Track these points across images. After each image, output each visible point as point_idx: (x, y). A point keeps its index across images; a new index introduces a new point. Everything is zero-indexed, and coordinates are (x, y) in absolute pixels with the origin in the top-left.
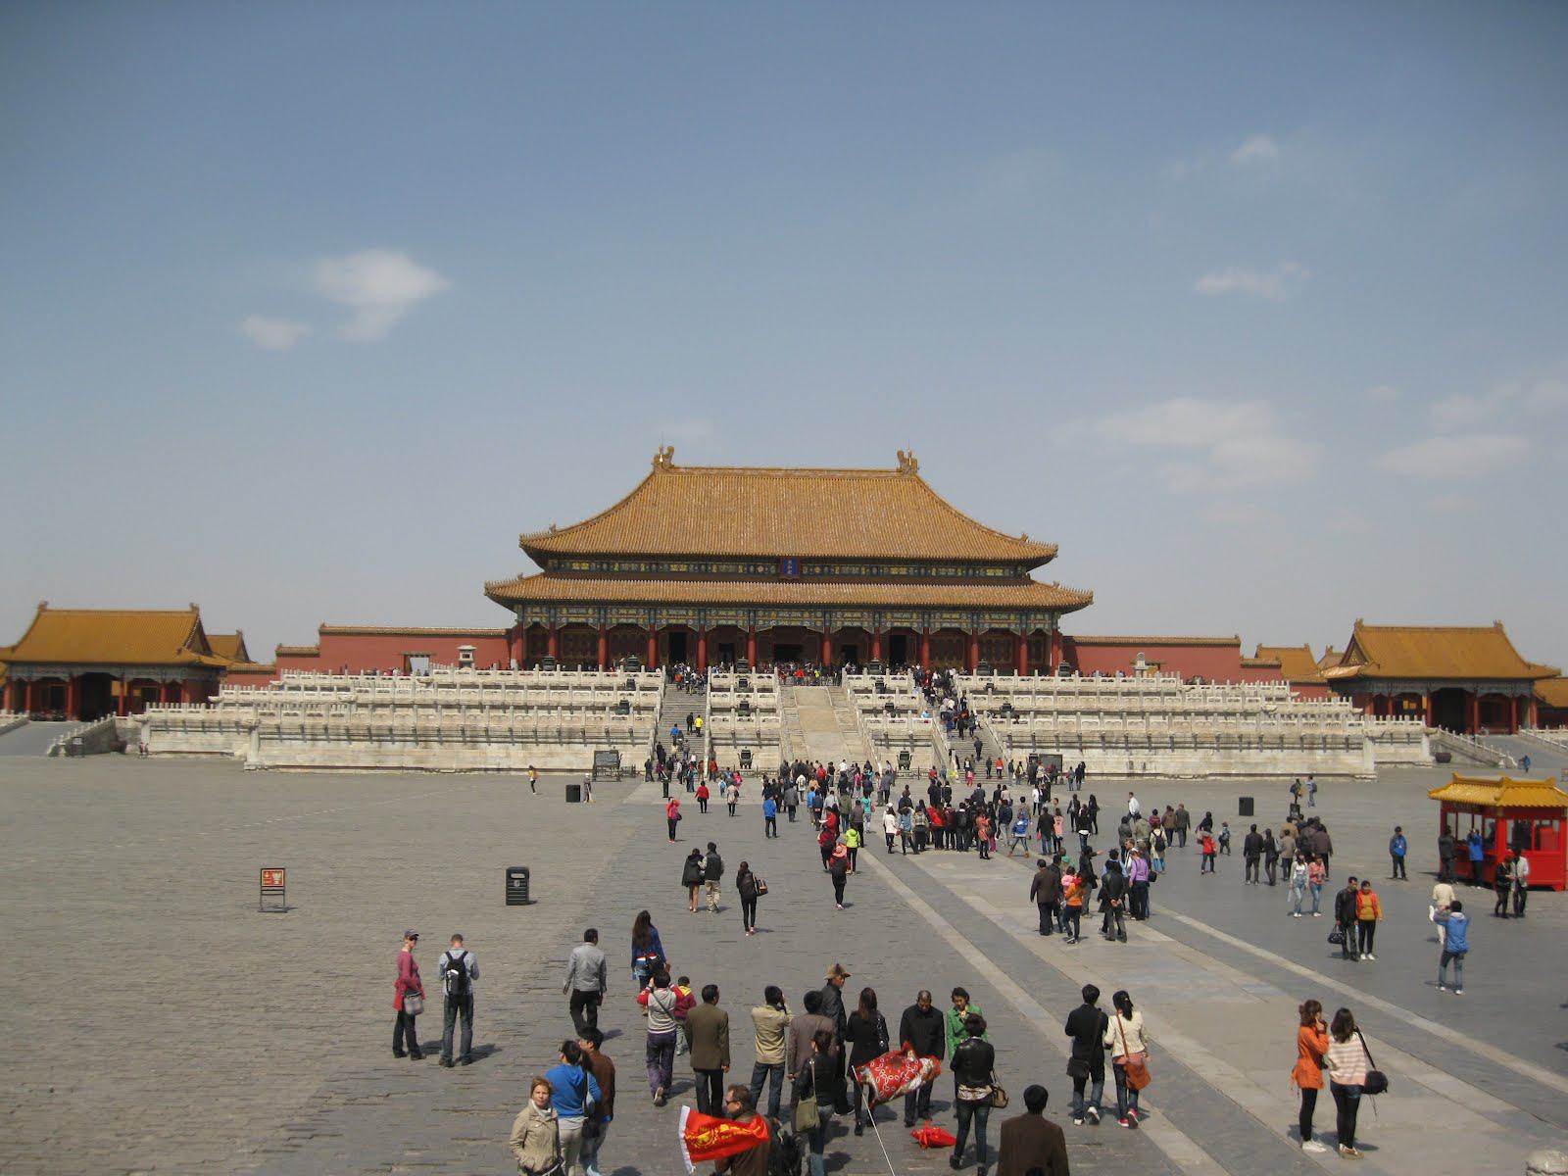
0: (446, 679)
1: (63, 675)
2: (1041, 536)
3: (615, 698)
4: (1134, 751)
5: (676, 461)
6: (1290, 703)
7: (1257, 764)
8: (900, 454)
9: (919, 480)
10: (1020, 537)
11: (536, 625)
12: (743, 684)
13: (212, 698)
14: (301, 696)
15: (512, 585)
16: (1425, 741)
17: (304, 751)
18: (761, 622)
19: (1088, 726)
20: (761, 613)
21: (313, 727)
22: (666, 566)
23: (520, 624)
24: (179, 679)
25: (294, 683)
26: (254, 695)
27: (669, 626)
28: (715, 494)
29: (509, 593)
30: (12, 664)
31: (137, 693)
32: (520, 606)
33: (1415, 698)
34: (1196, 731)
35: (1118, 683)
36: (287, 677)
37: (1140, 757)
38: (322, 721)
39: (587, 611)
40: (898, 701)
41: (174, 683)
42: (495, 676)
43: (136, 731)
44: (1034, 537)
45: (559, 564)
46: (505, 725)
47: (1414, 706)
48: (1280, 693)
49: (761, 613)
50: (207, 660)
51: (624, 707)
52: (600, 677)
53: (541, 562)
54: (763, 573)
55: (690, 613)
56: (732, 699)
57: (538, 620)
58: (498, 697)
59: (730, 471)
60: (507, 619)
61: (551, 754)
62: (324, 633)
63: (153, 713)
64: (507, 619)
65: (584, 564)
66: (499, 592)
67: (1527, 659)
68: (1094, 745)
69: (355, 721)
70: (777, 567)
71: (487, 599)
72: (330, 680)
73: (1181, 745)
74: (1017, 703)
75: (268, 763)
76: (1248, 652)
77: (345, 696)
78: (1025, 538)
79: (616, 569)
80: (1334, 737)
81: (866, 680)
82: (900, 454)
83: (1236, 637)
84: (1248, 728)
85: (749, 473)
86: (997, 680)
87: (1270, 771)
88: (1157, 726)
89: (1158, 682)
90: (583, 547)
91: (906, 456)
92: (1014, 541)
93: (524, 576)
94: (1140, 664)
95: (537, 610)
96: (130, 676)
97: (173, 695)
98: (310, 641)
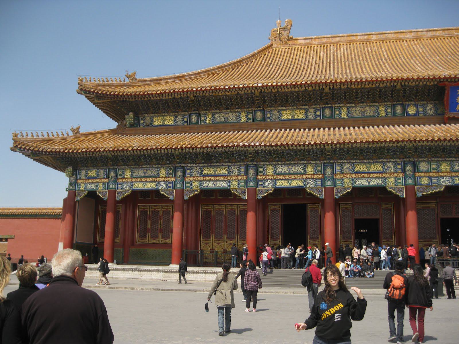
11: (92, 194)
15: (62, 140)
18: (425, 181)
20: (423, 166)
22: (275, 112)
23: (72, 194)
27: (278, 191)
32: (70, 169)
39: (158, 172)
45: (137, 117)
49: (423, 166)
54: (415, 115)
55: (310, 169)
57: (93, 187)
59: (354, 38)
65: (168, 118)
70: (435, 105)
71: (19, 156)
79: (209, 121)
85: (374, 37)
93: (81, 131)
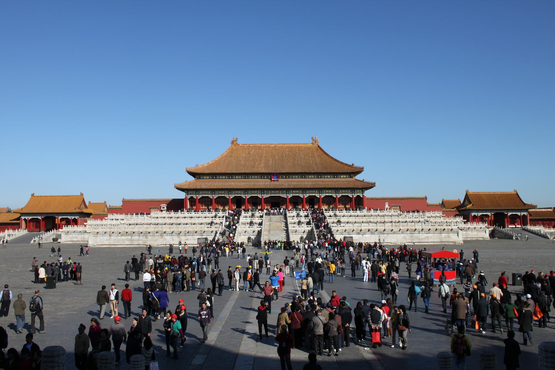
0: (156, 216)
1: (40, 218)
2: (358, 164)
3: (209, 220)
4: (380, 235)
5: (238, 142)
6: (442, 219)
8: (312, 138)
9: (319, 146)
11: (192, 197)
12: (253, 215)
13: (85, 224)
14: (114, 222)
16: (487, 231)
17: (107, 240)
19: (365, 227)
21: (110, 232)
24: (76, 217)
25: (112, 218)
26: (99, 222)
28: (251, 153)
29: (182, 187)
30: (23, 214)
31: (63, 222)
33: (487, 216)
34: (401, 228)
35: (379, 212)
36: (110, 216)
37: (382, 237)
38: (113, 230)
40: (303, 220)
41: (75, 219)
42: (172, 214)
43: (61, 235)
44: (356, 165)
46: (172, 230)
47: (486, 219)
48: (438, 215)
50: (85, 211)
51: (212, 223)
52: (207, 214)
53: (194, 177)
56: (249, 220)
58: (171, 221)
60: (181, 195)
61: (187, 240)
62: (124, 202)
63: (65, 229)
66: (179, 187)
67: (525, 202)
69: (123, 230)
72: (123, 216)
74: (342, 220)
75: (95, 244)
76: (429, 201)
77: (122, 222)
78: (353, 165)
80: (448, 229)
81: (294, 213)
82: (312, 138)
84: (419, 227)
86: (338, 213)
87: (426, 241)
88: (388, 226)
89: (392, 212)
90: (207, 171)
92: (350, 166)
94: (387, 206)
96: (60, 217)
97: (75, 222)
98: (119, 204)
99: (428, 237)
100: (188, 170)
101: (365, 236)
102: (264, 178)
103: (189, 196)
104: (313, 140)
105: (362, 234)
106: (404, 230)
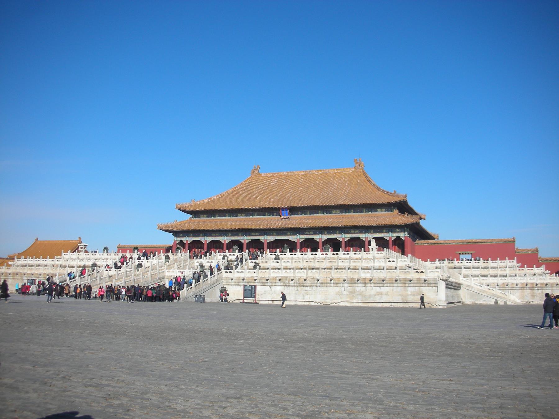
7: (370, 296)
8: (356, 160)
9: (363, 172)
10: (393, 192)
28: (272, 184)
29: (167, 229)
64: (170, 240)
66: (163, 229)
68: (277, 284)
73: (325, 285)
80: (419, 279)
82: (356, 160)
83: (514, 238)
90: (201, 208)
91: (358, 161)
95: (181, 235)
99: (381, 294)
100: (178, 206)
101: (274, 288)
102: (273, 215)
103: (179, 239)
104: (357, 163)
105: (271, 287)
106: (339, 279)
